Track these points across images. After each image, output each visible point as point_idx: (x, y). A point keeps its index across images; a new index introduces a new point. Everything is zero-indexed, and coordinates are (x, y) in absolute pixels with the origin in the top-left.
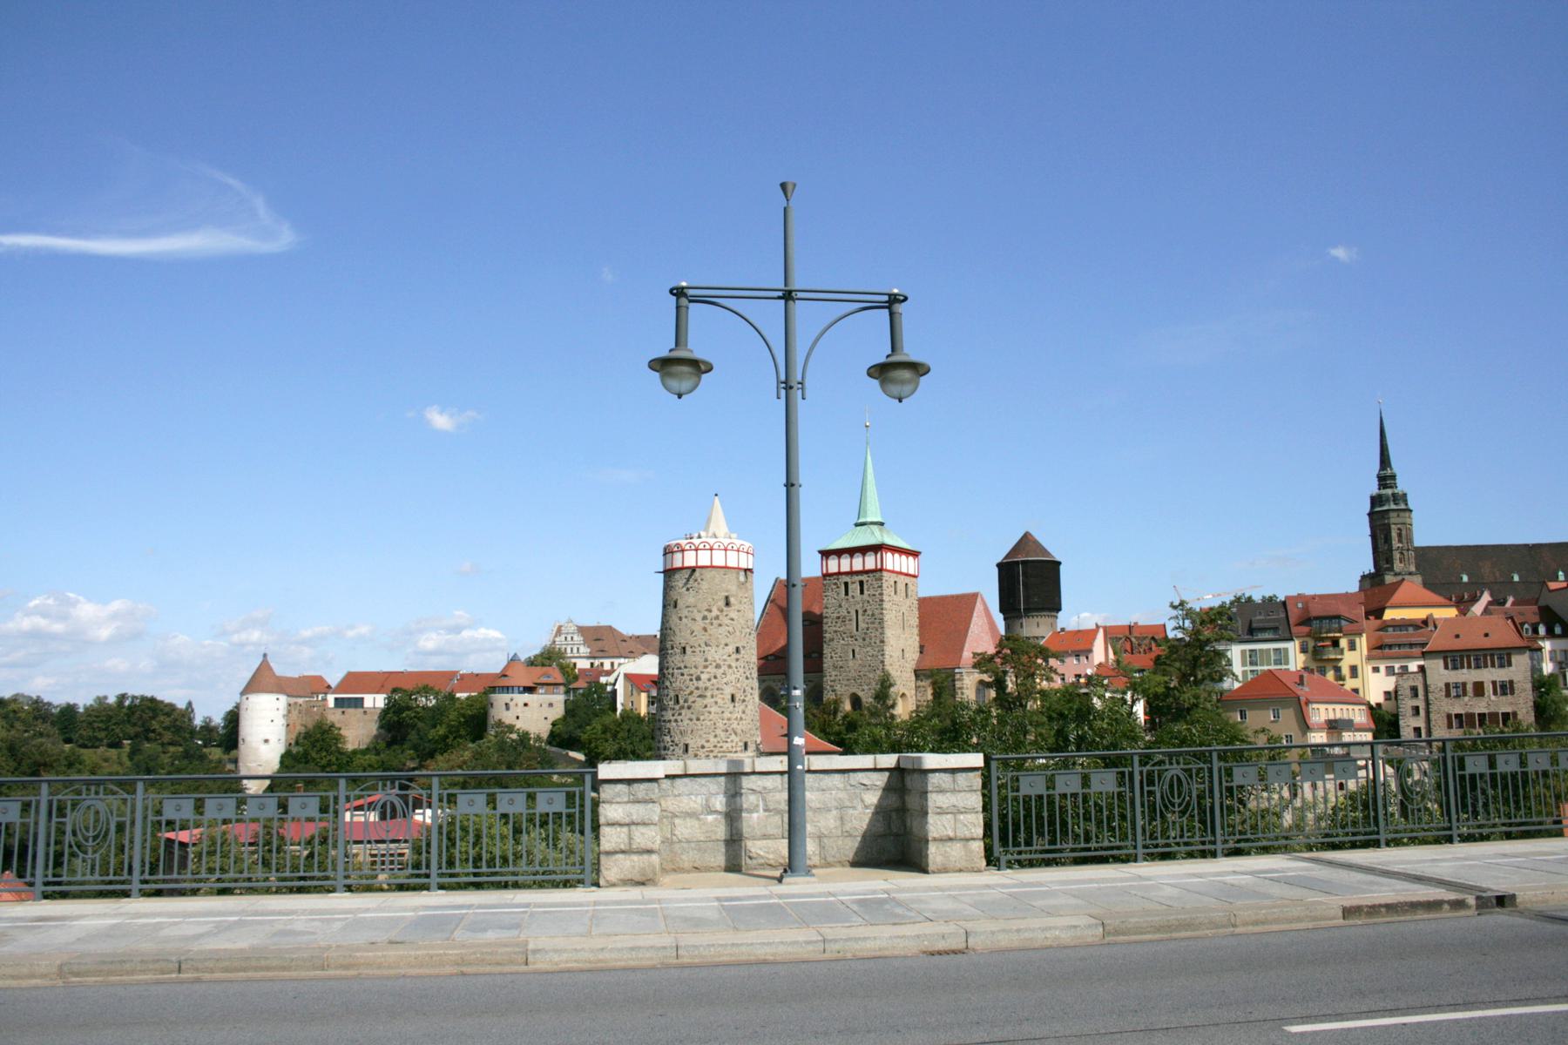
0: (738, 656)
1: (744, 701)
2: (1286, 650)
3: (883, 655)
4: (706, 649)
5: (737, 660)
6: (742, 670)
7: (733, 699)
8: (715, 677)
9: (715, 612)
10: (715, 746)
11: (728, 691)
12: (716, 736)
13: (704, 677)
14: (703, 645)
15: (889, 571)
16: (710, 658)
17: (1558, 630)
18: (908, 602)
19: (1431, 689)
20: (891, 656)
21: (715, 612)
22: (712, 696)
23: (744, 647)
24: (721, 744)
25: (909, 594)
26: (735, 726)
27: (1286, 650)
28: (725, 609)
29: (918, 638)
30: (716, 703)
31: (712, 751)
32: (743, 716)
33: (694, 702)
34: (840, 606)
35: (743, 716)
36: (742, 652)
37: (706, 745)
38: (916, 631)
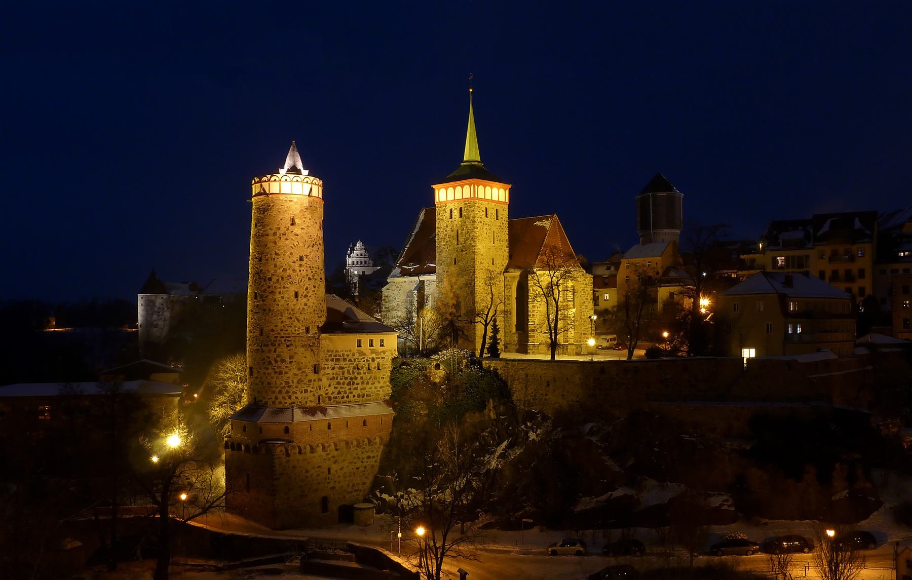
1: (306, 296)
2: (807, 257)
3: (474, 262)
5: (301, 265)
6: (304, 273)
7: (296, 295)
8: (282, 278)
9: (283, 230)
10: (282, 330)
11: (292, 289)
12: (282, 322)
13: (274, 279)
15: (481, 199)
16: (278, 264)
18: (498, 223)
20: (481, 263)
21: (281, 232)
22: (280, 293)
23: (307, 256)
24: (286, 328)
26: (297, 315)
28: (291, 227)
29: (507, 250)
30: (283, 298)
32: (306, 307)
34: (447, 226)
35: (306, 307)
36: (305, 259)
37: (274, 328)
38: (507, 243)
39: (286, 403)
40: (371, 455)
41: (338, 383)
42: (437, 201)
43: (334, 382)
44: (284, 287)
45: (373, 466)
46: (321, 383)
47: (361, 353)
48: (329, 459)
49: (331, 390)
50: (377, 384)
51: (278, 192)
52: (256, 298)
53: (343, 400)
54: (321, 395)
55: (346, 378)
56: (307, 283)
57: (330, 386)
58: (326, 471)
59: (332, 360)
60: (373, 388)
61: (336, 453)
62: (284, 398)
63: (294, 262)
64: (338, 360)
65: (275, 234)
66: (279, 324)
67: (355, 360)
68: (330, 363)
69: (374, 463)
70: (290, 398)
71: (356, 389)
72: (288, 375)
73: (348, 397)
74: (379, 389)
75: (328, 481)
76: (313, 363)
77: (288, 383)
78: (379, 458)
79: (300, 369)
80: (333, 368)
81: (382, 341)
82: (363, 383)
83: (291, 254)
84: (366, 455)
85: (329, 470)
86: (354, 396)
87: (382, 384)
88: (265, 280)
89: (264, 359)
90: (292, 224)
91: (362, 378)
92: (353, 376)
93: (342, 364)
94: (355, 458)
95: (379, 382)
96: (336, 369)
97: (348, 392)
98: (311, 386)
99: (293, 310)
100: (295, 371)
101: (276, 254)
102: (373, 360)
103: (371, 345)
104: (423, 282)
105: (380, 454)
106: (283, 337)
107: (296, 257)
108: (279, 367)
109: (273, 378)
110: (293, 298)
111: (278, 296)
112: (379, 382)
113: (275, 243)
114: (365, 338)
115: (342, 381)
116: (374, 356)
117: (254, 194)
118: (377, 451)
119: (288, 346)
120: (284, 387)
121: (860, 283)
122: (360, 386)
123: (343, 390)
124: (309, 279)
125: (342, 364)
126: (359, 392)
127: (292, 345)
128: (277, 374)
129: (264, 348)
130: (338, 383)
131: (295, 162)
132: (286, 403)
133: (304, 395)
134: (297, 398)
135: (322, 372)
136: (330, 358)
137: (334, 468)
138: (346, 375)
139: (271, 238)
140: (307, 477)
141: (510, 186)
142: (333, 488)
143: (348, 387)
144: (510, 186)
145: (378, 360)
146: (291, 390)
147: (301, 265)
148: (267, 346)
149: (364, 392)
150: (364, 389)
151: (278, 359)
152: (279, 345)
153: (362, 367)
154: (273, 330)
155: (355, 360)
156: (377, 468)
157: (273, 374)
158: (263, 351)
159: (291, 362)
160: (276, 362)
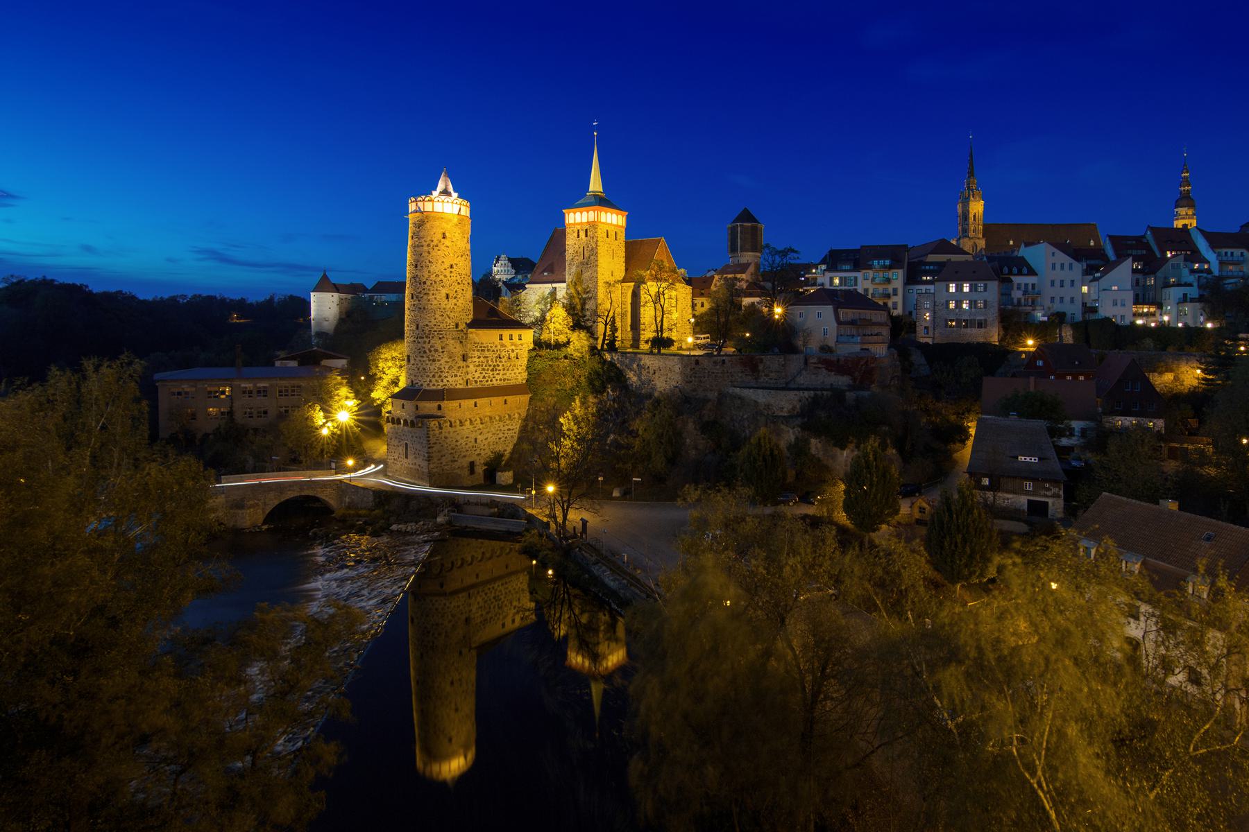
0: (452, 270)
1: (456, 297)
3: (597, 273)
4: (430, 264)
5: (451, 272)
6: (454, 279)
8: (435, 282)
9: (435, 242)
11: (444, 292)
12: (435, 319)
13: (428, 283)
14: (427, 261)
15: (603, 223)
16: (432, 270)
17: (1025, 270)
18: (617, 243)
19: (937, 304)
21: (435, 243)
22: (433, 294)
23: (456, 264)
24: (439, 324)
25: (618, 237)
27: (856, 278)
28: (442, 240)
29: (624, 265)
31: (432, 328)
32: (455, 307)
33: (422, 297)
34: (575, 244)
35: (455, 307)
37: (429, 324)
38: (624, 259)
39: (439, 385)
40: (511, 428)
41: (484, 370)
42: (567, 222)
43: (480, 368)
44: (437, 290)
45: (512, 437)
46: (468, 369)
47: (503, 345)
48: (476, 431)
49: (477, 375)
50: (516, 371)
51: (431, 210)
52: (412, 298)
53: (488, 383)
54: (469, 379)
55: (490, 366)
56: (457, 287)
57: (476, 371)
58: (473, 440)
59: (478, 351)
60: (513, 374)
61: (481, 426)
62: (436, 381)
63: (445, 269)
64: (482, 350)
65: (429, 245)
66: (433, 320)
67: (497, 350)
68: (476, 353)
69: (514, 434)
70: (442, 381)
71: (498, 374)
72: (440, 363)
73: (491, 381)
74: (517, 374)
75: (475, 449)
77: (441, 368)
78: (517, 430)
79: (450, 358)
80: (479, 357)
81: (520, 336)
82: (504, 370)
83: (443, 262)
84: (506, 428)
85: (476, 440)
86: (497, 380)
87: (520, 371)
88: (420, 284)
89: (419, 349)
90: (444, 238)
91: (503, 365)
92: (495, 364)
93: (486, 353)
94: (498, 430)
95: (518, 369)
96: (482, 359)
97: (491, 376)
98: (460, 371)
99: (444, 309)
100: (447, 359)
101: (430, 262)
102: (513, 351)
103: (511, 339)
104: (556, 288)
105: (518, 427)
106: (436, 331)
107: (447, 265)
108: (433, 356)
109: (427, 364)
110: (444, 299)
111: (431, 297)
112: (518, 369)
113: (429, 253)
114: (506, 333)
115: (486, 368)
116: (513, 347)
117: (410, 211)
118: (516, 425)
119: (440, 338)
120: (437, 373)
121: (894, 299)
122: (502, 372)
123: (487, 375)
124: (459, 283)
125: (486, 353)
126: (501, 376)
127: (443, 337)
128: (431, 362)
129: (420, 340)
130: (484, 370)
131: (446, 186)
132: (439, 385)
133: (454, 379)
134: (448, 381)
135: (470, 360)
136: (476, 349)
137: (480, 438)
138: (490, 363)
139: (425, 248)
140: (457, 446)
141: (627, 213)
142: (479, 454)
143: (491, 373)
144: (627, 213)
145: (517, 351)
146: (443, 375)
147: (451, 272)
148: (423, 338)
149: (505, 377)
150: (505, 374)
151: (432, 349)
152: (433, 337)
153: (504, 357)
154: (427, 325)
155: (497, 350)
156: (516, 439)
157: (427, 362)
158: (419, 342)
159: (443, 352)
160: (430, 351)
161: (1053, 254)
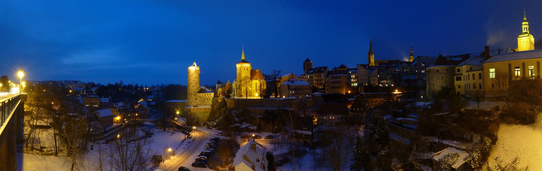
11: (192, 86)
56: (194, 84)
76: (195, 98)
93: (201, 98)
114: (206, 94)
121: (322, 81)
161: (361, 67)
